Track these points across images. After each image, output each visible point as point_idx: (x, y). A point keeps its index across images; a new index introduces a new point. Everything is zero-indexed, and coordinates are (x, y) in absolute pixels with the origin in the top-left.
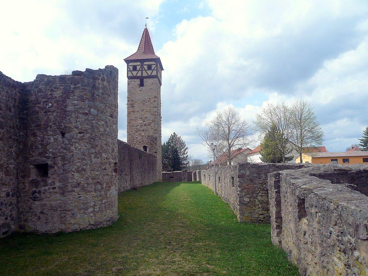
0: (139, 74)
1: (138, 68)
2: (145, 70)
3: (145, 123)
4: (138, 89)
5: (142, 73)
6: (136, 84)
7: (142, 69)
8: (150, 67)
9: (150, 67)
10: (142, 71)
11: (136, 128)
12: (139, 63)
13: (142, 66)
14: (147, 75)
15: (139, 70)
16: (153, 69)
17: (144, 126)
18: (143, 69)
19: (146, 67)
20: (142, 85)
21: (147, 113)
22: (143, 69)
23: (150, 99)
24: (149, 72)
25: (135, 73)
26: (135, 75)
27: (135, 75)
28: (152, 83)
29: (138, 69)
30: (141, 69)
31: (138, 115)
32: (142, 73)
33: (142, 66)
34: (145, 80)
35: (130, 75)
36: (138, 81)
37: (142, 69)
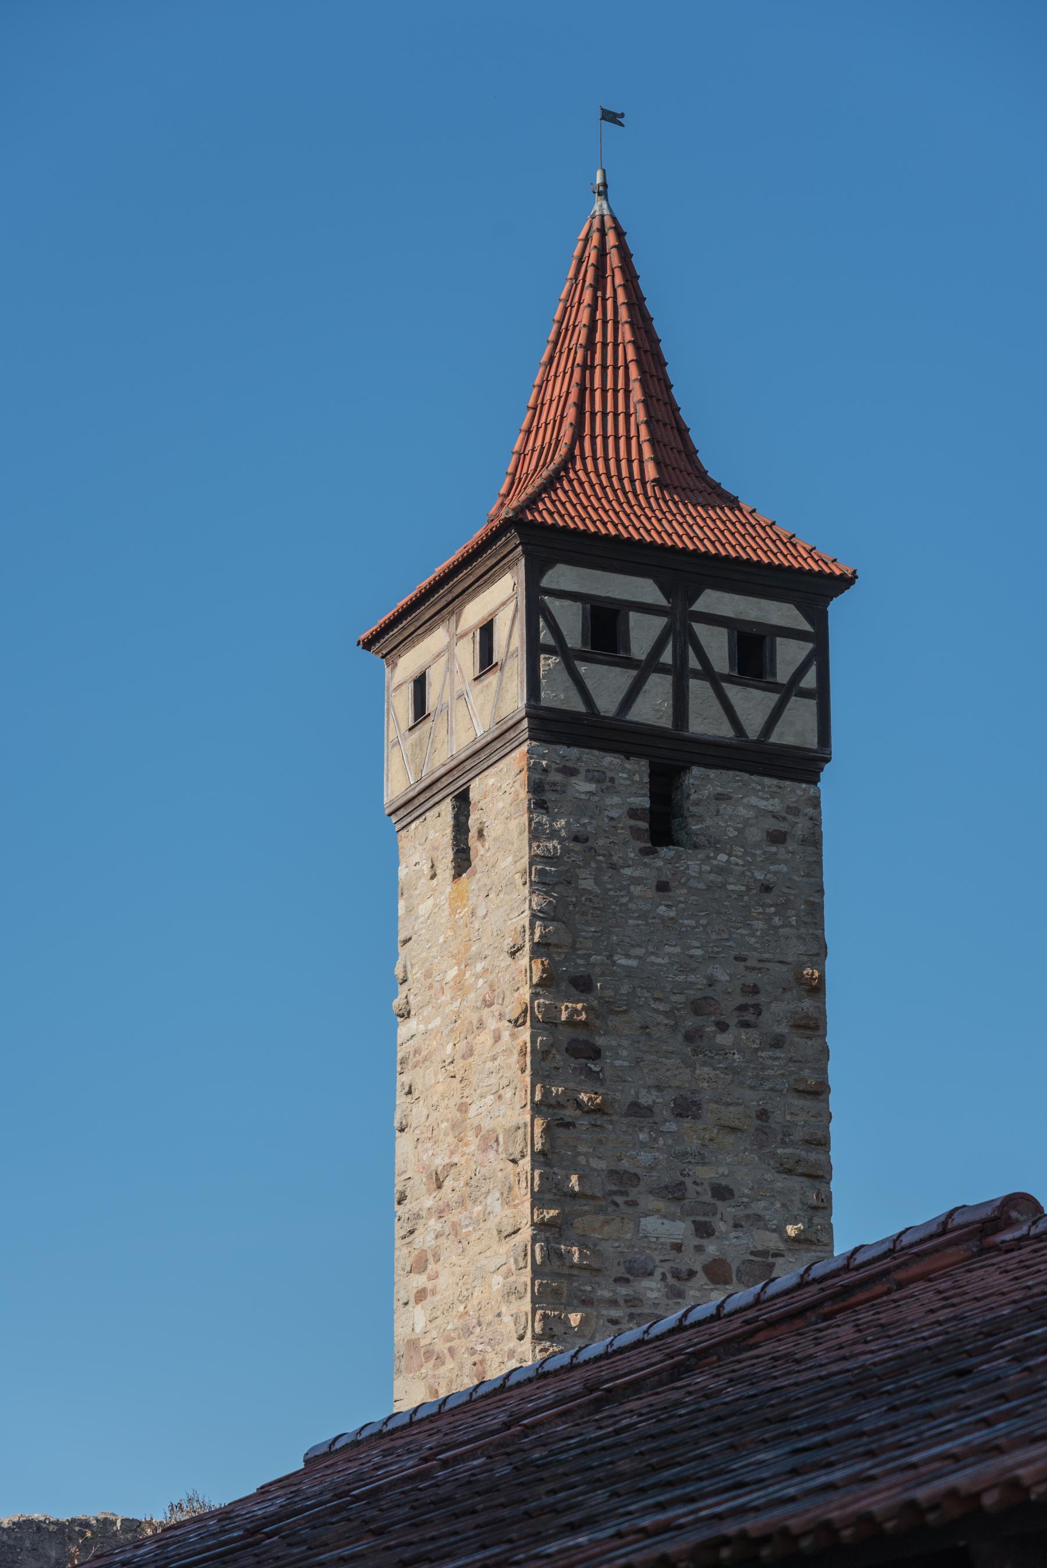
1: (643, 634)
2: (708, 673)
3: (712, 1249)
4: (639, 870)
6: (615, 805)
7: (681, 657)
10: (680, 675)
11: (623, 1290)
12: (645, 590)
13: (680, 630)
15: (651, 665)
16: (783, 676)
17: (701, 1279)
18: (694, 663)
21: (730, 1139)
22: (694, 663)
23: (755, 990)
24: (752, 705)
25: (607, 685)
26: (607, 704)
28: (772, 824)
29: (640, 645)
30: (667, 657)
31: (645, 1157)
33: (680, 630)
37: (681, 657)
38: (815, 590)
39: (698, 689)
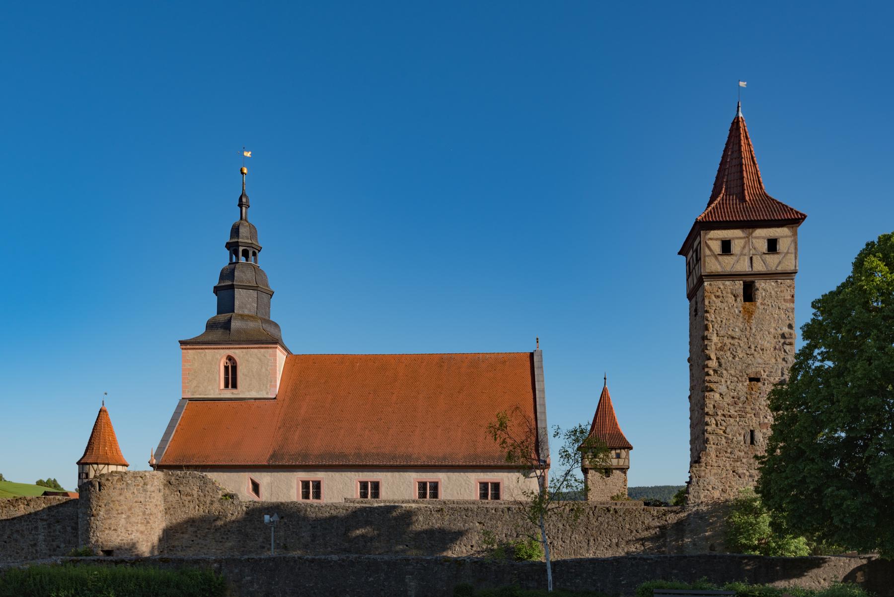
0: (743, 266)
1: (736, 247)
20: (749, 294)
27: (728, 269)
34: (760, 284)
36: (739, 286)
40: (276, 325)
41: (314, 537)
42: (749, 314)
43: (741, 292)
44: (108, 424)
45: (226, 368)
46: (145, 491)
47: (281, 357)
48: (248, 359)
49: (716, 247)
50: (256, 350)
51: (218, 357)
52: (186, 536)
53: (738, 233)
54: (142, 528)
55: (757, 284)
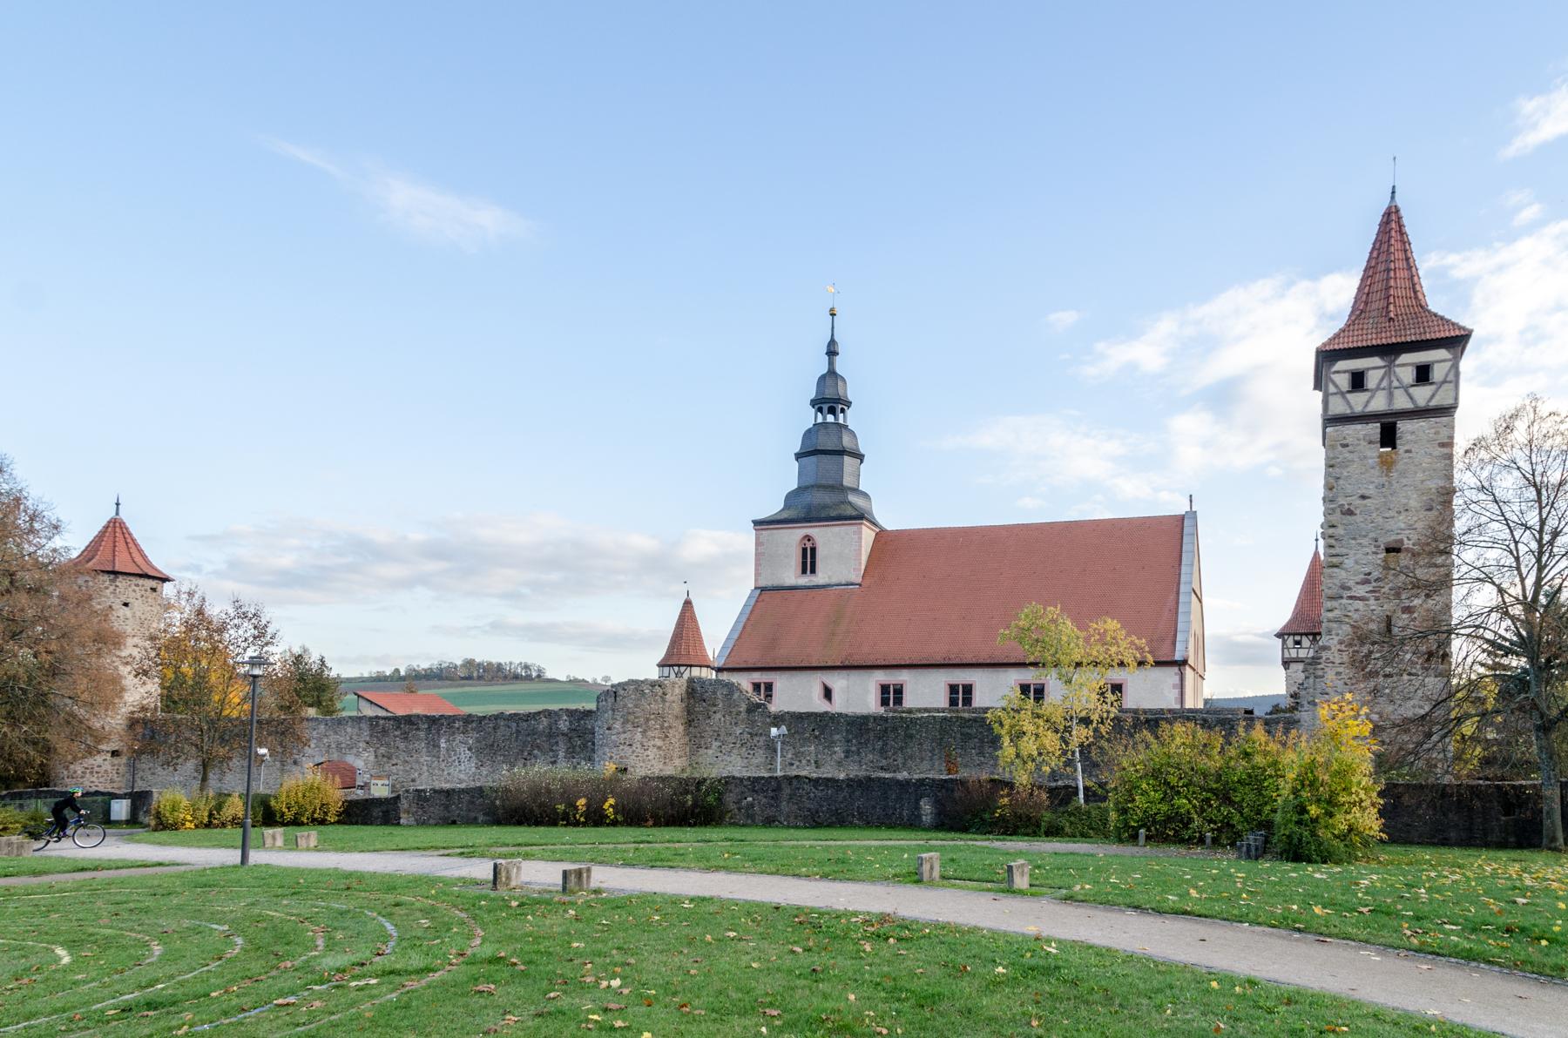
0: (1379, 404)
1: (1372, 380)
5: (1391, 396)
8: (1423, 374)
9: (1423, 374)
14: (1409, 406)
15: (1378, 388)
19: (1408, 375)
22: (1395, 383)
24: (1422, 395)
27: (1358, 409)
30: (1385, 384)
32: (1391, 396)
34: (1403, 426)
35: (1338, 407)
36: (1374, 429)
38: (1457, 341)
39: (1399, 394)
40: (865, 495)
41: (847, 753)
42: (1387, 464)
43: (1378, 437)
44: (694, 619)
45: (804, 550)
46: (664, 701)
47: (868, 535)
48: (826, 537)
49: (1344, 381)
50: (836, 529)
51: (792, 538)
52: (710, 752)
53: (1376, 361)
54: (659, 743)
55: (1400, 424)
